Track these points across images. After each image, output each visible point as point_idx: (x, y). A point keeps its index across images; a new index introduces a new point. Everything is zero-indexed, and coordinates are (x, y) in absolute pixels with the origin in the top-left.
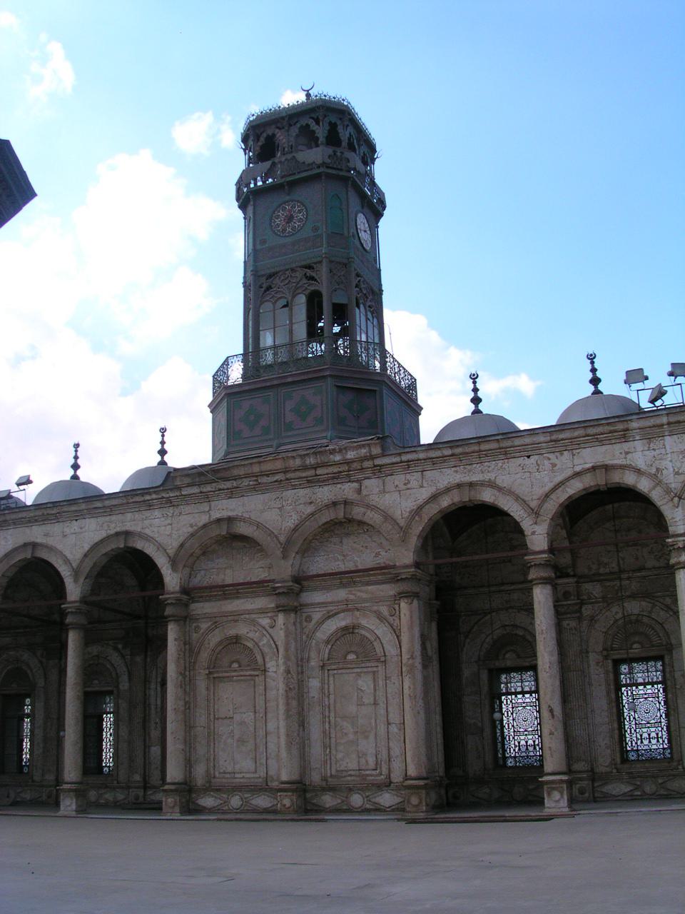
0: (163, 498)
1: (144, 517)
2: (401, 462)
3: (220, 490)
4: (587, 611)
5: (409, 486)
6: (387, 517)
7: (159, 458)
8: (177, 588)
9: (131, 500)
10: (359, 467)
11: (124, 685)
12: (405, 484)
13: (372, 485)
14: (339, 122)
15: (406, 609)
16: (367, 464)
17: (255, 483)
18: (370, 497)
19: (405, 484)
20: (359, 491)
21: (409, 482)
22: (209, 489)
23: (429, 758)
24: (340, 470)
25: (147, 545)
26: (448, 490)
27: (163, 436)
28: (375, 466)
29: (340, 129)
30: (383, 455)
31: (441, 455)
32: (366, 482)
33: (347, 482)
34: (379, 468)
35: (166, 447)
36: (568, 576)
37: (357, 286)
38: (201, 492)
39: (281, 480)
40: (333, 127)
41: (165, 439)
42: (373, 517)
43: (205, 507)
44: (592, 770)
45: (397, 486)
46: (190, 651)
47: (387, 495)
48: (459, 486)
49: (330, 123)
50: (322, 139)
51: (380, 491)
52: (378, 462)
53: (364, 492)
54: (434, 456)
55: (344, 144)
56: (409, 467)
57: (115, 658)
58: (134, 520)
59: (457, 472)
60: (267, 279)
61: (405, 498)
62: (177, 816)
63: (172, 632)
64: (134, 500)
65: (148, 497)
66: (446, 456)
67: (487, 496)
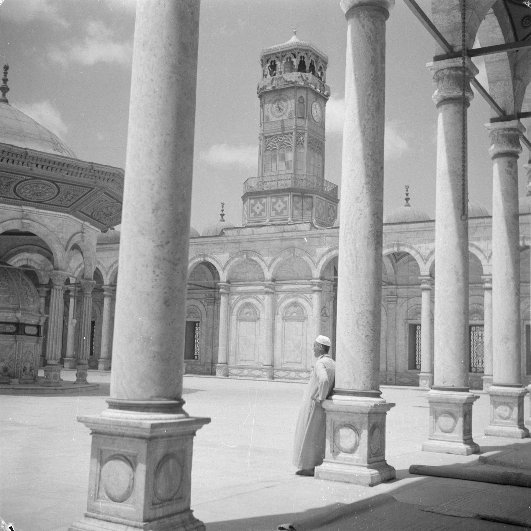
4: (400, 301)
8: (225, 280)
11: (204, 319)
14: (305, 56)
15: (316, 297)
46: (230, 308)
50: (296, 67)
55: (307, 68)
57: (201, 307)
62: (222, 376)
63: (223, 299)
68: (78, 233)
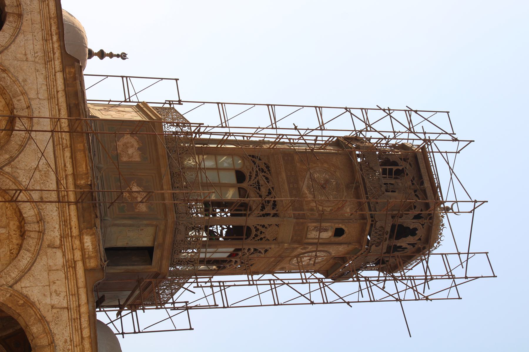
0: (54, 54)
1: (35, 34)
2: (78, 288)
3: (59, 110)
5: (54, 294)
6: (25, 272)
7: (96, 50)
9: (52, 22)
10: (75, 247)
12: (56, 291)
13: (57, 259)
16: (78, 255)
17: (64, 145)
18: (45, 257)
19: (56, 291)
20: (51, 246)
21: (58, 295)
22: (60, 100)
24: (73, 228)
25: (7, 35)
26: (49, 333)
27: (118, 56)
28: (75, 262)
29: (410, 239)
31: (83, 326)
32: (59, 254)
33: (61, 235)
34: (73, 265)
35: (107, 58)
37: (255, 250)
38: (58, 92)
39: (66, 170)
40: (413, 232)
41: (115, 58)
42: (25, 258)
43: (43, 94)
45: (54, 283)
47: (45, 274)
49: (416, 229)
51: (50, 266)
52: (80, 265)
53: (50, 251)
54: (83, 320)
56: (72, 295)
58: (32, 24)
59: (66, 342)
60: (265, 164)
64: (53, 24)
65: (55, 38)
66: (81, 332)
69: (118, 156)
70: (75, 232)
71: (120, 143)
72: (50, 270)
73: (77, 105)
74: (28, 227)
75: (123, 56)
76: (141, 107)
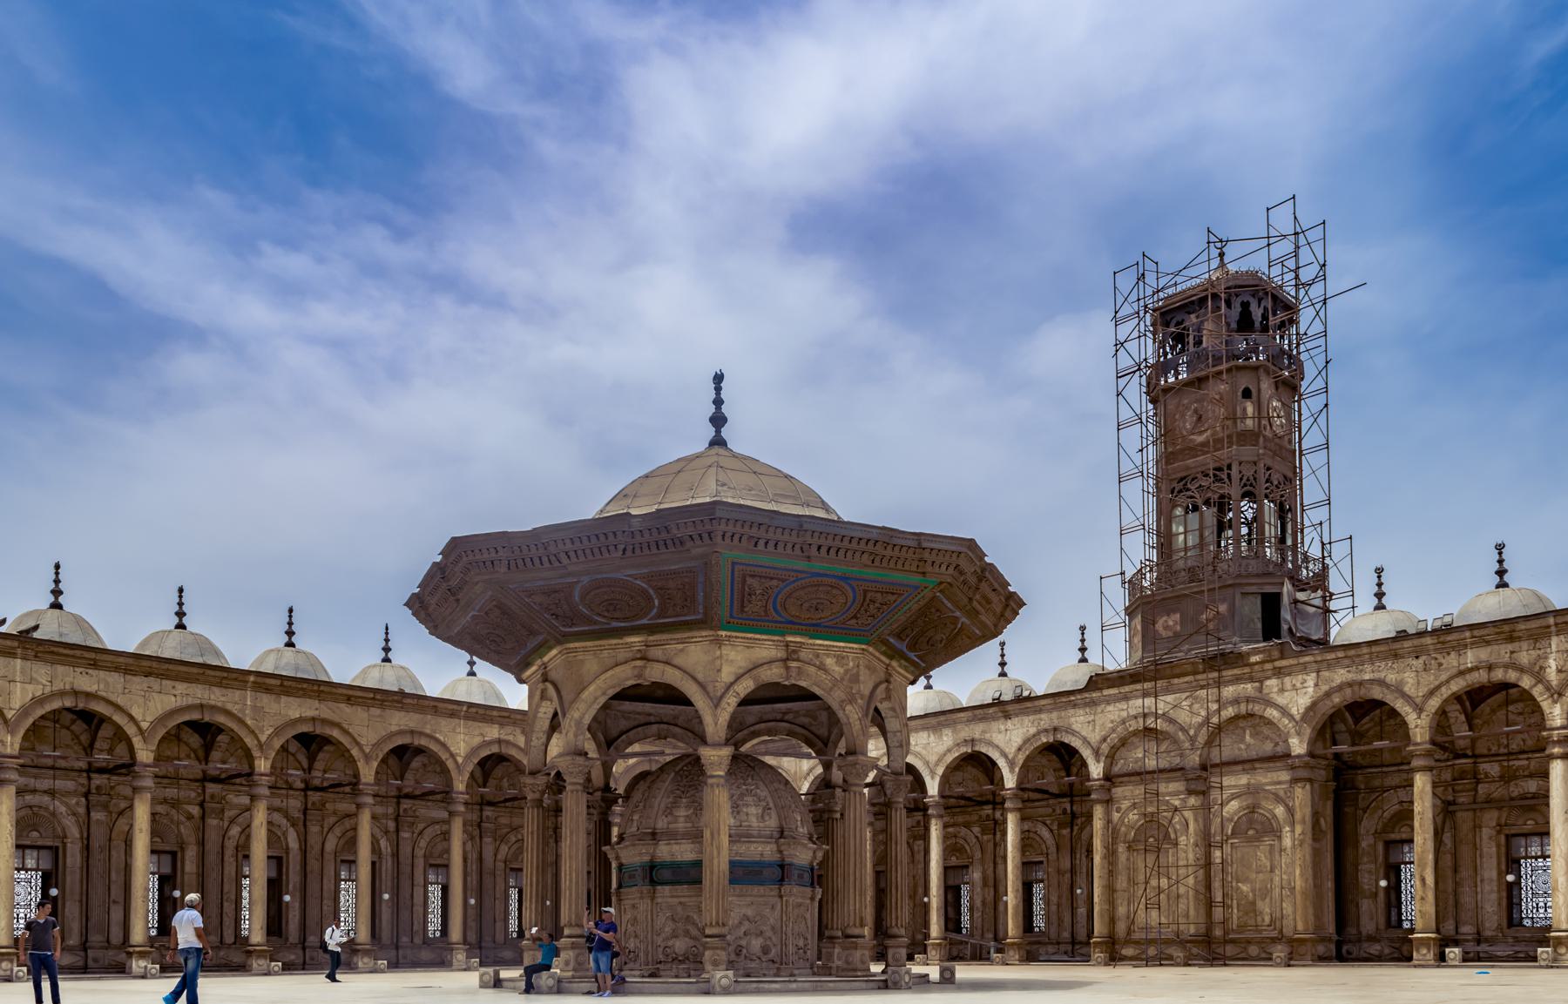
6: (1284, 711)
13: (1272, 683)
16: (1268, 666)
20: (1260, 690)
23: (1318, 916)
26: (1340, 688)
30: (1282, 658)
32: (1268, 683)
36: (1466, 756)
42: (1272, 713)
44: (1478, 933)
48: (1350, 684)
53: (1265, 691)
61: (1297, 695)
67: (1377, 693)
68: (881, 683)
69: (1176, 635)
70: (1247, 670)
71: (1164, 634)
72: (1282, 690)
73: (1131, 676)
74: (1243, 711)
75: (1083, 629)
76: (1130, 612)
